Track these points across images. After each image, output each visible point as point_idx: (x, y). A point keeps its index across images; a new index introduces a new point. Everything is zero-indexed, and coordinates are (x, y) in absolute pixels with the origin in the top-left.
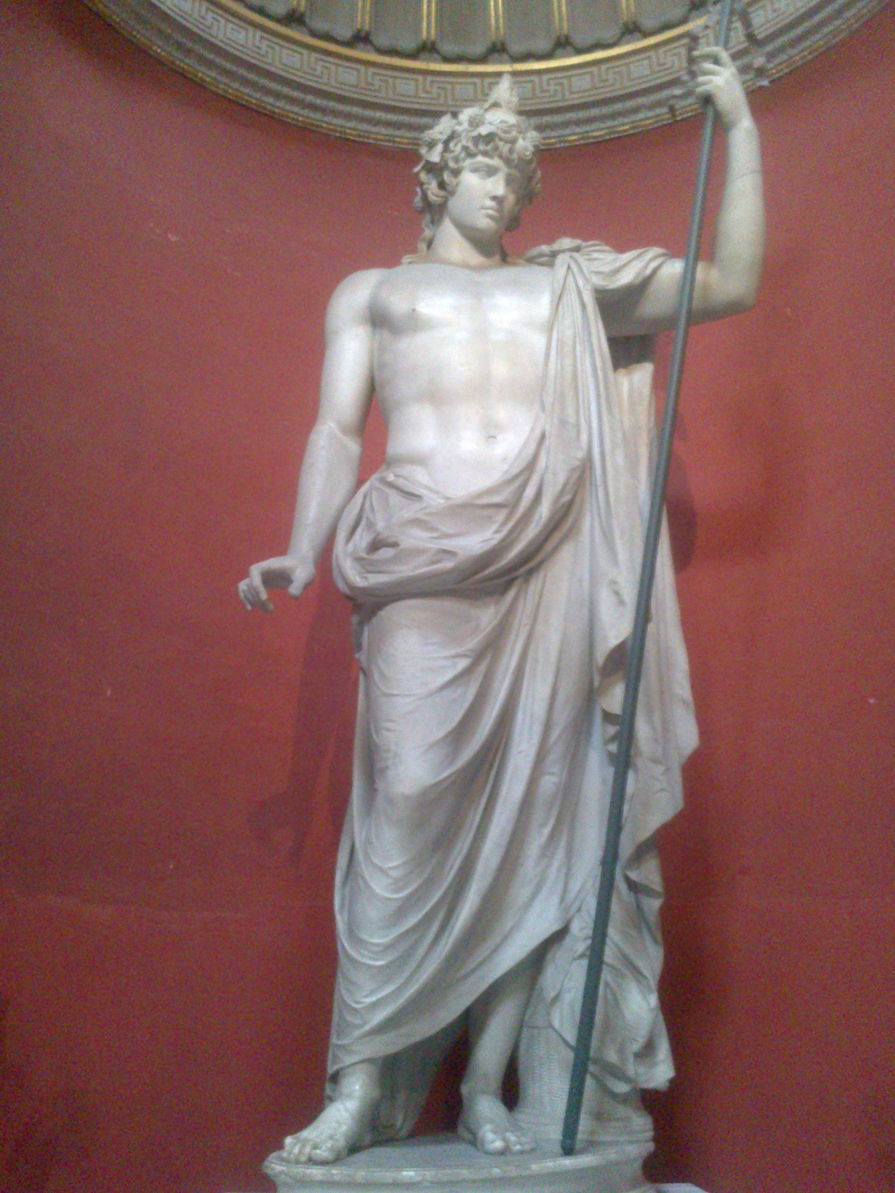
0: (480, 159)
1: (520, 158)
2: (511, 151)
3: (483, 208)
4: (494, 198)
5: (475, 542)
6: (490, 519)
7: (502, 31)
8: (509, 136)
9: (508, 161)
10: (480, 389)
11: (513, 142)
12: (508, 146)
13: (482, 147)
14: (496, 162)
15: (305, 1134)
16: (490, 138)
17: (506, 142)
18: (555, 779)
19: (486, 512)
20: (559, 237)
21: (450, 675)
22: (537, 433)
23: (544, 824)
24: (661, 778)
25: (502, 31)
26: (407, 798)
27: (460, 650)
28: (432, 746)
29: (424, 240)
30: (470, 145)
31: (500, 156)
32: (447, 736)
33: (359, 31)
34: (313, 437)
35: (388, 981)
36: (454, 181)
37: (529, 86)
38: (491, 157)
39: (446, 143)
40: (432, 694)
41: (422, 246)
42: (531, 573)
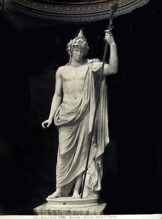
0: (76, 49)
2: (80, 47)
5: (71, 118)
6: (73, 114)
10: (73, 92)
11: (81, 45)
15: (51, 195)
16: (77, 46)
18: (84, 150)
21: (68, 137)
22: (81, 99)
26: (62, 155)
27: (70, 134)
32: (66, 147)
35: (61, 177)
40: (65, 141)
42: (80, 121)
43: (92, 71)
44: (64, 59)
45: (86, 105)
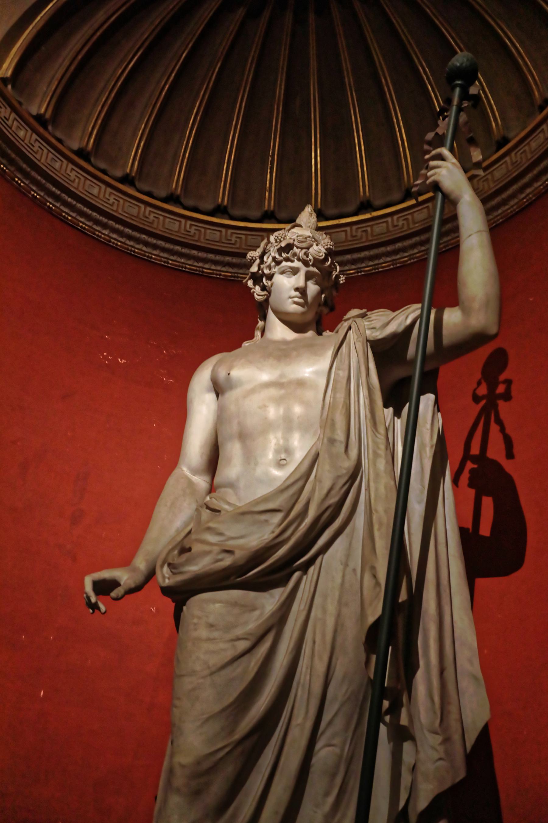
0: (284, 264)
1: (314, 258)
2: (306, 254)
3: (290, 298)
4: (297, 289)
7: (367, 194)
8: (304, 245)
9: (306, 263)
12: (304, 251)
13: (284, 255)
14: (297, 264)
16: (289, 247)
17: (302, 249)
19: (263, 517)
20: (350, 310)
23: (327, 794)
24: (438, 748)
25: (367, 194)
26: (183, 766)
28: (207, 720)
29: (258, 328)
30: (277, 256)
31: (299, 260)
32: (224, 710)
33: (266, 212)
34: (170, 478)
36: (269, 283)
37: (384, 225)
38: (292, 261)
39: (261, 257)
40: (212, 674)
41: (258, 333)
43: (367, 341)
44: (234, 317)
45: (339, 477)
